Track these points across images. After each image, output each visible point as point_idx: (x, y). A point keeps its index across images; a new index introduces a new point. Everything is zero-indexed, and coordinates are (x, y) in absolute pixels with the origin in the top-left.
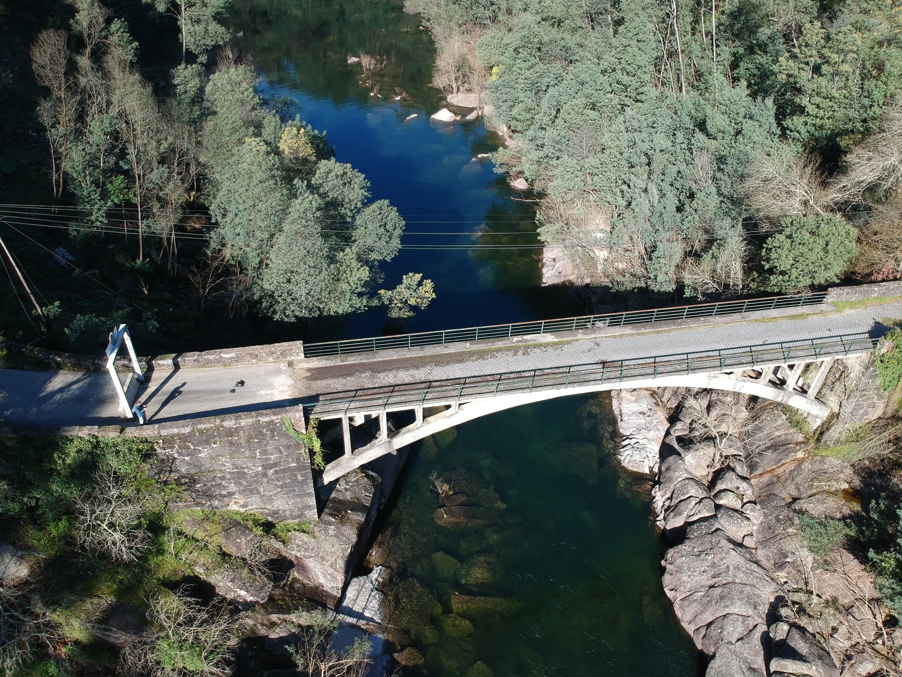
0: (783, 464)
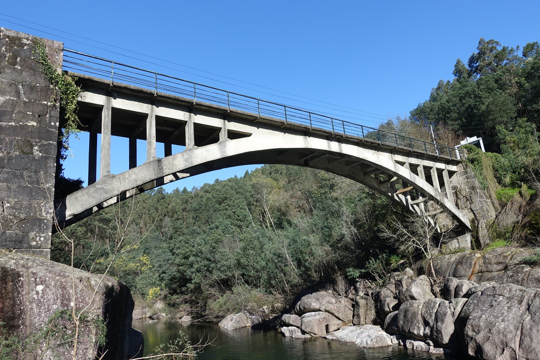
0: (475, 264)
